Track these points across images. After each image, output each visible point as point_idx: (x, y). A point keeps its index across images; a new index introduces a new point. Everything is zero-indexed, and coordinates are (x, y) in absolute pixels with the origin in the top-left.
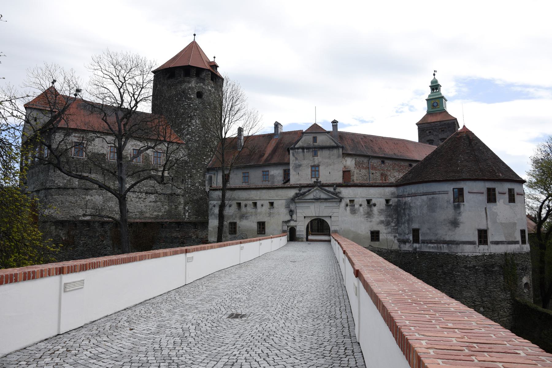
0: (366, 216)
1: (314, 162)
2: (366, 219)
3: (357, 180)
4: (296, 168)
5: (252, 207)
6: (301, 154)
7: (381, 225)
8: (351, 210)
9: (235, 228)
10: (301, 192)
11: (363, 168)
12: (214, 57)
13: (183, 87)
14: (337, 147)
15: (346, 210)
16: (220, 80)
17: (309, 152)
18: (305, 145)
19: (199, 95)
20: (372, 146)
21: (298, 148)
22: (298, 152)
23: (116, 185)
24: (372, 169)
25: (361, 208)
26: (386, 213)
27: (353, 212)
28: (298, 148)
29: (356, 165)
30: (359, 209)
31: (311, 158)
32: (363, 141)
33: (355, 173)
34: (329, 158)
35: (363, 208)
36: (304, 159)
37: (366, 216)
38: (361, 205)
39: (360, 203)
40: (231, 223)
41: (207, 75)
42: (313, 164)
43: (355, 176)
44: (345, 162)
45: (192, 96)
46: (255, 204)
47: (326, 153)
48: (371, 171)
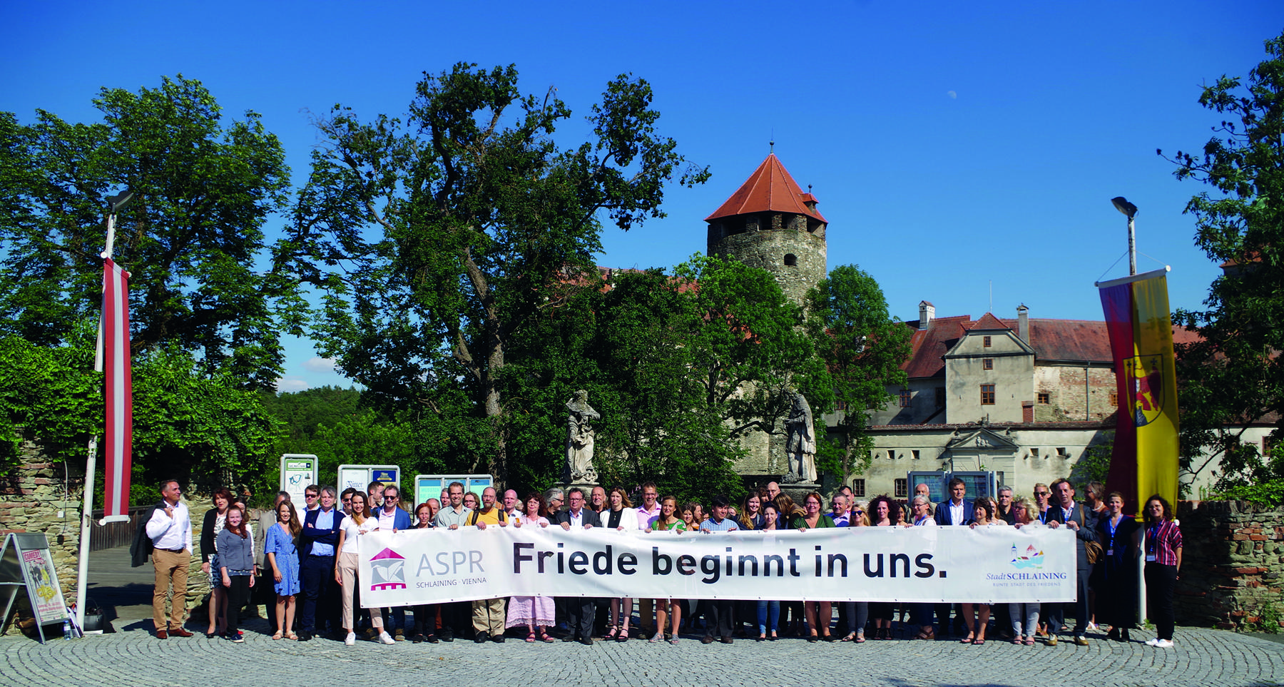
1: (987, 379)
3: (1064, 404)
4: (957, 388)
5: (888, 457)
6: (965, 366)
8: (1033, 462)
9: (863, 488)
10: (959, 436)
11: (1075, 383)
12: (810, 187)
13: (761, 248)
14: (1026, 354)
15: (1025, 463)
16: (822, 226)
17: (977, 362)
18: (972, 351)
19: (790, 260)
20: (1095, 343)
21: (959, 357)
22: (959, 362)
24: (1092, 385)
27: (1036, 466)
28: (959, 357)
29: (1061, 378)
30: (1045, 463)
31: (981, 371)
32: (1077, 335)
33: (1060, 394)
34: (1012, 371)
36: (970, 374)
39: (1047, 453)
40: (856, 481)
41: (801, 223)
42: (984, 382)
43: (1059, 398)
44: (1042, 374)
45: (777, 264)
46: (892, 454)
47: (1006, 362)
48: (1091, 388)
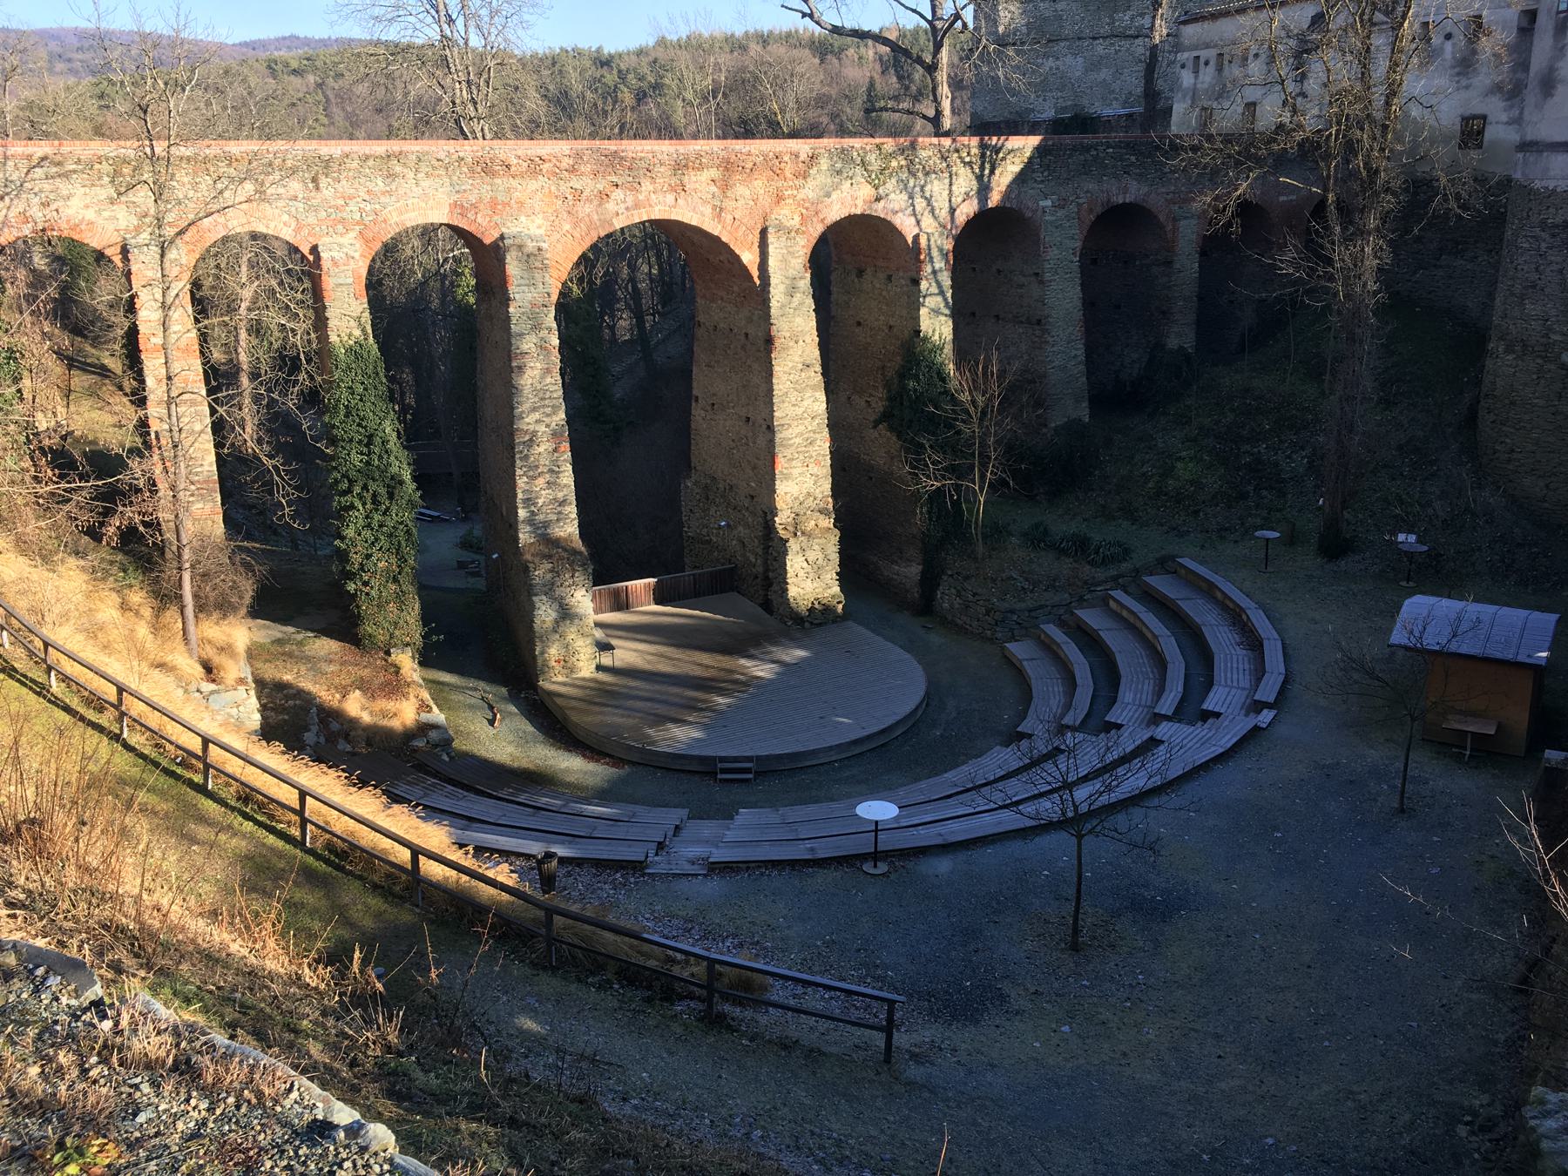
0: (1457, 70)
2: (1457, 79)
7: (1493, 99)
23: (1117, 23)
25: (1448, 46)
26: (1515, 55)
30: (1442, 49)
35: (1454, 45)
37: (1457, 70)
38: (1448, 37)
